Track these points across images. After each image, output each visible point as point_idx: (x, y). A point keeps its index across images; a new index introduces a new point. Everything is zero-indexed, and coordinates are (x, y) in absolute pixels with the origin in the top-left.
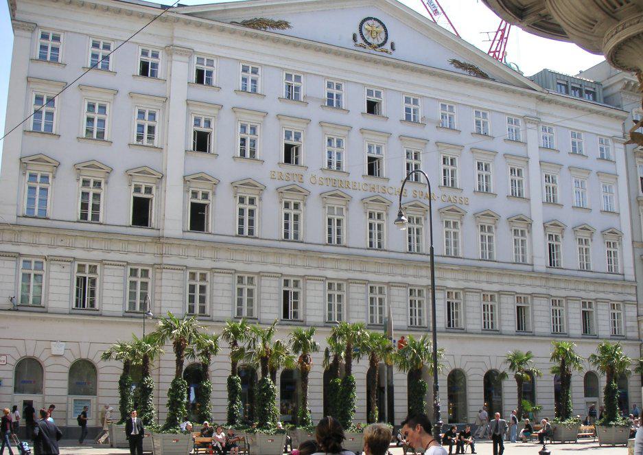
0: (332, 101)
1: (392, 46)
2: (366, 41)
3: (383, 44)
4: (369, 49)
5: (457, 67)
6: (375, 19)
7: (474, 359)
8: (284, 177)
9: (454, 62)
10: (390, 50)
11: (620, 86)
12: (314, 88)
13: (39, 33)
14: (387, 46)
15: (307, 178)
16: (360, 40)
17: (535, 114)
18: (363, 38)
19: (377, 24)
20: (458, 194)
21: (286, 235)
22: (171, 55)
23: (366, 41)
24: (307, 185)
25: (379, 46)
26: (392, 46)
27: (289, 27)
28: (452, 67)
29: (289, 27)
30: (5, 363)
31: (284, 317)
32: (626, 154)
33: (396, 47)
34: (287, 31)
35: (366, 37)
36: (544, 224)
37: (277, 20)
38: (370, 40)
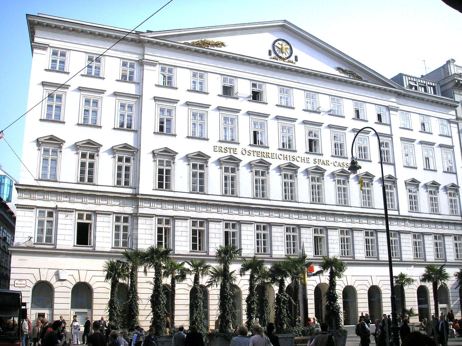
0: (256, 96)
1: (296, 57)
3: (289, 57)
5: (341, 73)
6: (283, 40)
7: (360, 278)
8: (223, 150)
10: (294, 61)
11: (452, 84)
12: (244, 89)
13: (50, 51)
14: (292, 58)
15: (239, 151)
16: (273, 55)
18: (276, 53)
22: (143, 66)
23: (277, 55)
24: (239, 156)
25: (287, 58)
26: (296, 57)
27: (224, 45)
28: (337, 73)
29: (224, 45)
30: (25, 286)
33: (299, 59)
34: (223, 49)
35: (277, 52)
37: (215, 42)
38: (280, 55)
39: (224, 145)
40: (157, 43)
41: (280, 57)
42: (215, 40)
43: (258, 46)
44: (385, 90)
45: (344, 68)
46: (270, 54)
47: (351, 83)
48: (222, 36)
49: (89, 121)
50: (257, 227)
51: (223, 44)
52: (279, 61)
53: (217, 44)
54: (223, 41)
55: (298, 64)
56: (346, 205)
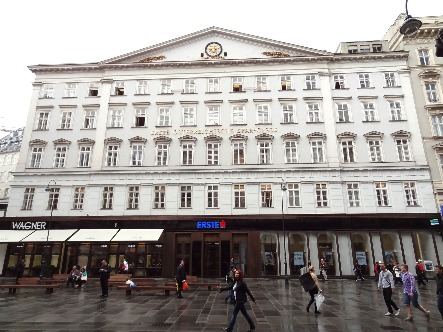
2: (209, 55)
4: (210, 59)
9: (266, 53)
14: (222, 55)
16: (205, 55)
17: (327, 70)
18: (207, 54)
19: (216, 45)
20: (269, 127)
21: (134, 164)
23: (209, 55)
28: (265, 56)
32: (411, 80)
34: (164, 60)
35: (209, 53)
39: (159, 130)
42: (157, 56)
44: (314, 60)
45: (271, 51)
46: (202, 55)
47: (277, 61)
48: (162, 51)
49: (65, 126)
51: (163, 57)
52: (210, 59)
53: (158, 58)
54: (163, 55)
55: (226, 58)
56: (316, 162)
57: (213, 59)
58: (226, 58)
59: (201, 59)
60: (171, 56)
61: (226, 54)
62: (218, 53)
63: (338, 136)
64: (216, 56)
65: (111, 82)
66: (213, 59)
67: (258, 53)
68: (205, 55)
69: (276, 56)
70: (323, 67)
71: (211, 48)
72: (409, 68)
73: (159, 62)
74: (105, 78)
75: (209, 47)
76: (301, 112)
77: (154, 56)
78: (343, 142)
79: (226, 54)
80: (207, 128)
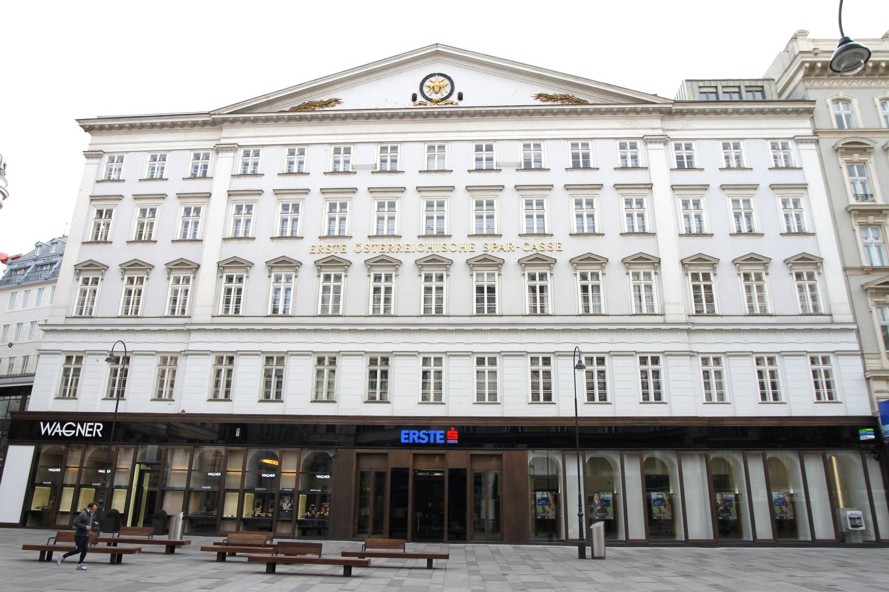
2: (427, 98)
3: (447, 97)
4: (429, 105)
9: (539, 96)
12: (366, 156)
14: (454, 98)
16: (420, 98)
17: (660, 132)
19: (441, 78)
20: (546, 240)
21: (275, 310)
23: (427, 98)
27: (339, 103)
28: (538, 102)
31: (644, 399)
32: (820, 156)
34: (338, 107)
35: (427, 95)
36: (682, 261)
39: (325, 243)
40: (245, 121)
41: (431, 100)
42: (326, 99)
43: (397, 92)
46: (414, 98)
50: (425, 359)
51: (337, 101)
53: (327, 104)
55: (461, 104)
57: (436, 106)
58: (461, 104)
59: (411, 104)
60: (352, 99)
61: (460, 97)
62: (445, 95)
63: (682, 263)
64: (443, 100)
65: (232, 148)
66: (436, 106)
67: (524, 95)
68: (420, 98)
69: (559, 102)
70: (652, 126)
71: (432, 85)
72: (815, 134)
73: (329, 111)
74: (223, 141)
75: (427, 83)
76: (610, 212)
77: (318, 99)
78: (692, 274)
79: (460, 97)
80: (422, 241)
